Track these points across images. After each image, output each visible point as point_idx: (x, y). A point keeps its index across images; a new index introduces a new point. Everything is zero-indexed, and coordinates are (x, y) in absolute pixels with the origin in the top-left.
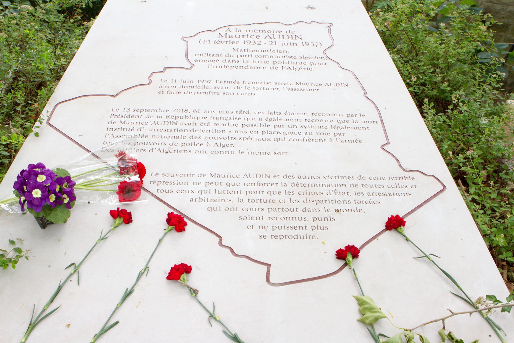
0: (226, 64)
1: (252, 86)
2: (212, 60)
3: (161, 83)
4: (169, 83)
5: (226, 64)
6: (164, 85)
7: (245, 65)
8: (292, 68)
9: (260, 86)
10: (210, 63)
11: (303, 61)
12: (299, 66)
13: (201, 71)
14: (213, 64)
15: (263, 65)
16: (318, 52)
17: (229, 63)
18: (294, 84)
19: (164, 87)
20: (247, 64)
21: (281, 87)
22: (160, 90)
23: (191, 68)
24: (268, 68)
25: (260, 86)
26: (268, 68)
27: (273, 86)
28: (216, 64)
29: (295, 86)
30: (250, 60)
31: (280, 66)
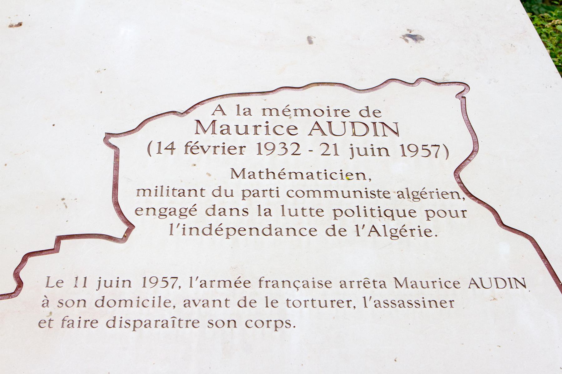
0: (215, 221)
1: (282, 294)
2: (177, 208)
3: (46, 291)
4: (68, 292)
5: (215, 221)
6: (55, 294)
7: (262, 222)
8: (381, 230)
9: (303, 294)
10: (174, 219)
11: (407, 204)
12: (397, 223)
13: (155, 248)
14: (182, 221)
15: (308, 222)
16: (437, 174)
17: (222, 219)
18: (390, 283)
19: (53, 304)
20: (268, 220)
21: (355, 294)
22: (43, 314)
23: (125, 237)
24: (321, 232)
25: (303, 294)
26: (321, 232)
27: (335, 293)
28: (190, 222)
29: (392, 293)
30: (273, 203)
31: (348, 223)
